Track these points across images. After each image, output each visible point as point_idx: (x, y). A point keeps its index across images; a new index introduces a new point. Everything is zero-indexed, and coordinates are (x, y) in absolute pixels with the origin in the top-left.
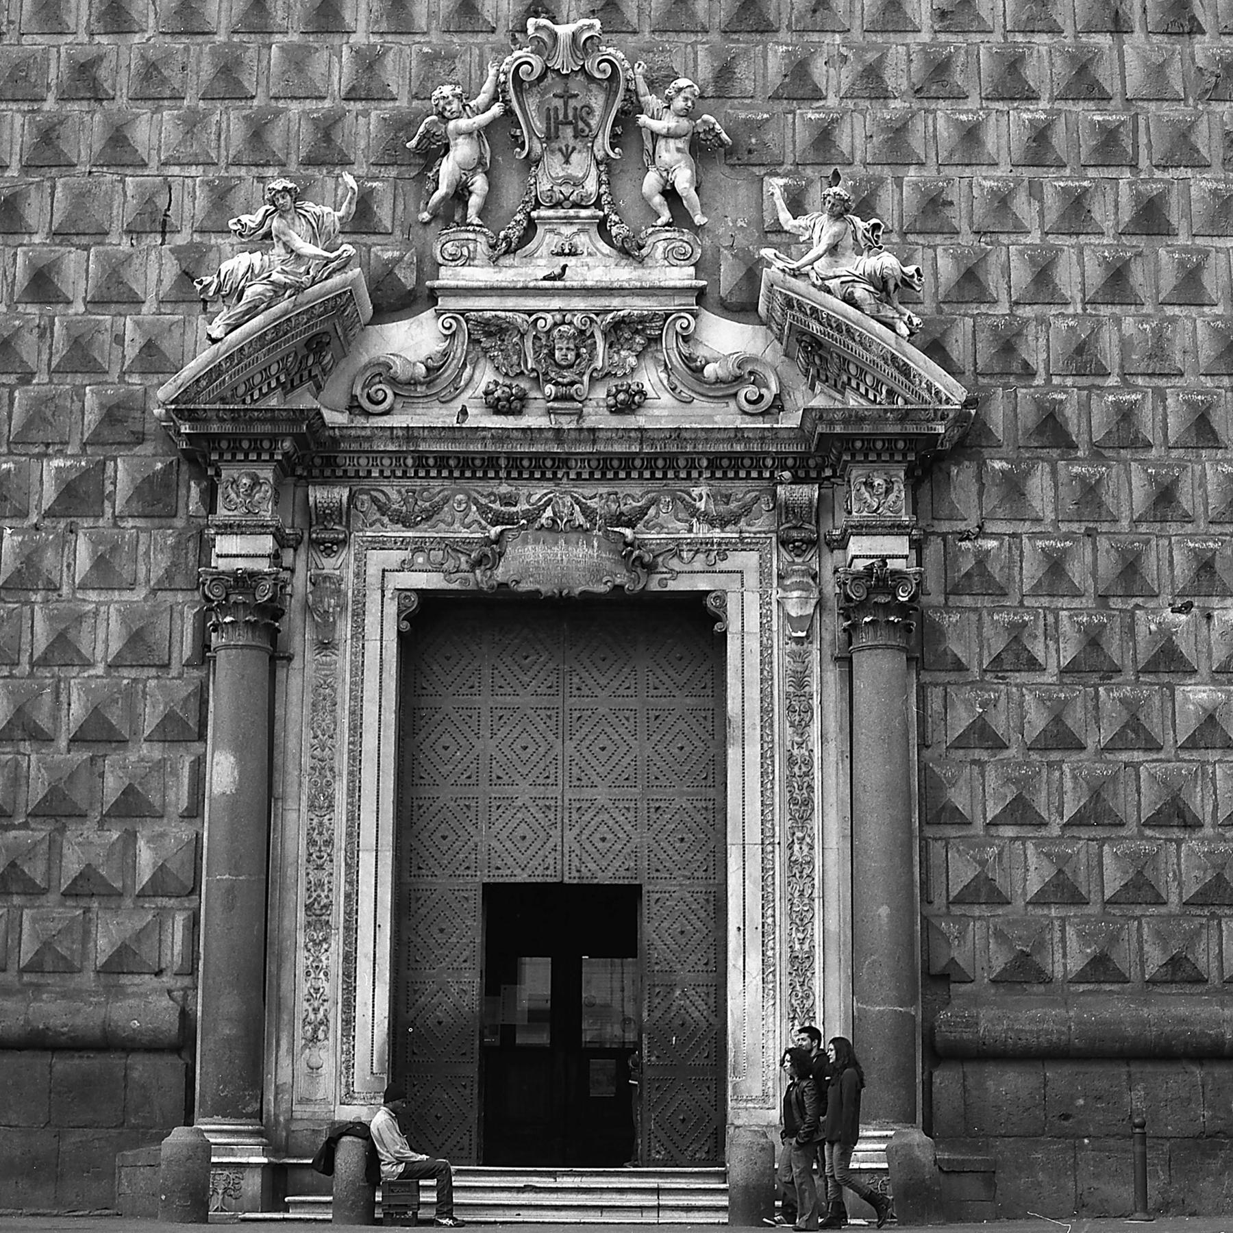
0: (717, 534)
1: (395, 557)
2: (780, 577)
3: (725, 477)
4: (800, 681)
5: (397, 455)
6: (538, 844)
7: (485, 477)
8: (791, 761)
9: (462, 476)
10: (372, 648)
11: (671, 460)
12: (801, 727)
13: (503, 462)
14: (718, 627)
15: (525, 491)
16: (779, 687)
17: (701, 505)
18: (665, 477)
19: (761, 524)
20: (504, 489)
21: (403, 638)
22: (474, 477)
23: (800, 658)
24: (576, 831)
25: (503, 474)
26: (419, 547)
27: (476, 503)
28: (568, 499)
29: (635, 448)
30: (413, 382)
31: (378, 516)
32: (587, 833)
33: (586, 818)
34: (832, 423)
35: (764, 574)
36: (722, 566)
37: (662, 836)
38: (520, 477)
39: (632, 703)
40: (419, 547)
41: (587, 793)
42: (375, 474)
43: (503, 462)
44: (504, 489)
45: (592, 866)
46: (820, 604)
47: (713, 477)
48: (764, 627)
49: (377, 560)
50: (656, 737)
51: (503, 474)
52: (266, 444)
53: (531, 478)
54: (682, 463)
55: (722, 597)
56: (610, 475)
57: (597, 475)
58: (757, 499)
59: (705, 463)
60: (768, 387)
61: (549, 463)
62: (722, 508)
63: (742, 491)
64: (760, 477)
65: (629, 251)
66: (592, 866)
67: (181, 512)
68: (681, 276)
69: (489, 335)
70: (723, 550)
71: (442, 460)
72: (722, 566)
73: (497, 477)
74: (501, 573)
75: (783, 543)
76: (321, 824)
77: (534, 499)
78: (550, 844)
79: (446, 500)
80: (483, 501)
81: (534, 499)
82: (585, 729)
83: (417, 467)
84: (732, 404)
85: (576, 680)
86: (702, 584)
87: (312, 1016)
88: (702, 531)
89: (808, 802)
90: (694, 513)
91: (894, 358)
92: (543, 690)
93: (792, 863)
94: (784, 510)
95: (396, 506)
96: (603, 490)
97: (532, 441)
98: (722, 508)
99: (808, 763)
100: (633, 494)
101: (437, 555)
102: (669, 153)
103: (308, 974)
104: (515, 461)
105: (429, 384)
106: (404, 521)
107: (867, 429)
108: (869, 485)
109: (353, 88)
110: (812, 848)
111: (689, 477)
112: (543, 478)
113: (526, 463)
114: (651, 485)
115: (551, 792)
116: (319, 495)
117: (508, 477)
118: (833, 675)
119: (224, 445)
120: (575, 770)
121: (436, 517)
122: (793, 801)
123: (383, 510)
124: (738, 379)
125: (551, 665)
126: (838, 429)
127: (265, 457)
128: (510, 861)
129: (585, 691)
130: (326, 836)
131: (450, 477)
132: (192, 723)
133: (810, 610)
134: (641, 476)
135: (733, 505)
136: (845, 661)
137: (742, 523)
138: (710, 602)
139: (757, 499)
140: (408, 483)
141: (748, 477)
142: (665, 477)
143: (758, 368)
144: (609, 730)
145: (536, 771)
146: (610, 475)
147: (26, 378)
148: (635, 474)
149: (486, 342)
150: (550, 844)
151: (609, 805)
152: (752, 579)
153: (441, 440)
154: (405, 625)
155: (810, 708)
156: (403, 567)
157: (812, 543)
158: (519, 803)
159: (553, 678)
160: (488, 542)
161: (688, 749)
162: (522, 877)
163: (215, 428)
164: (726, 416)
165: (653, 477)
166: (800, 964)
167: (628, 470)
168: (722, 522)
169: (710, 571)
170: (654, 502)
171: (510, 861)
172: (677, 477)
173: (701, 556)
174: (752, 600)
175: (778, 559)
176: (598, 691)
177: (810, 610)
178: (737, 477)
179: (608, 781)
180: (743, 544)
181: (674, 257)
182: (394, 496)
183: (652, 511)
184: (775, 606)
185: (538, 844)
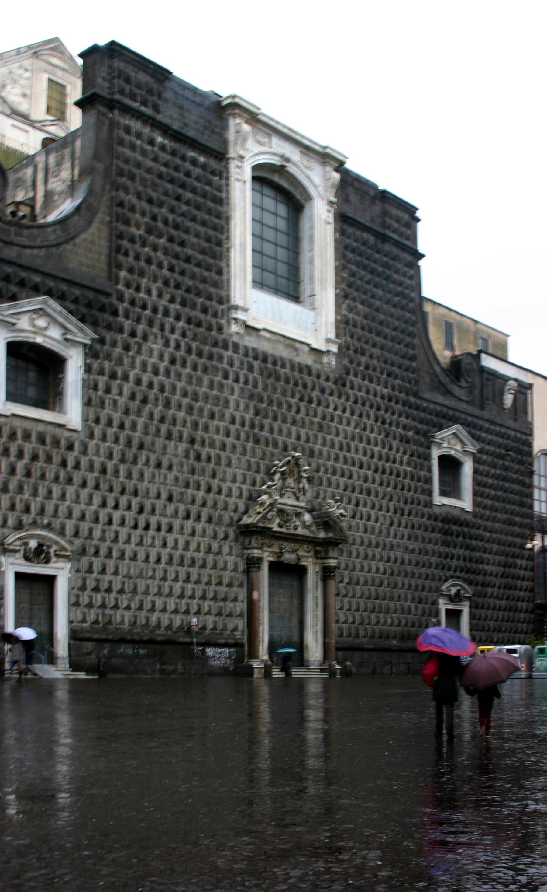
19: (312, 553)
26: (271, 552)
40: (271, 552)
49: (266, 554)
63: (310, 547)
65: (298, 499)
68: (303, 504)
74: (282, 559)
88: (306, 554)
94: (316, 552)
100: (297, 546)
102: (304, 481)
147: (217, 510)
156: (268, 556)
168: (308, 552)
181: (303, 501)
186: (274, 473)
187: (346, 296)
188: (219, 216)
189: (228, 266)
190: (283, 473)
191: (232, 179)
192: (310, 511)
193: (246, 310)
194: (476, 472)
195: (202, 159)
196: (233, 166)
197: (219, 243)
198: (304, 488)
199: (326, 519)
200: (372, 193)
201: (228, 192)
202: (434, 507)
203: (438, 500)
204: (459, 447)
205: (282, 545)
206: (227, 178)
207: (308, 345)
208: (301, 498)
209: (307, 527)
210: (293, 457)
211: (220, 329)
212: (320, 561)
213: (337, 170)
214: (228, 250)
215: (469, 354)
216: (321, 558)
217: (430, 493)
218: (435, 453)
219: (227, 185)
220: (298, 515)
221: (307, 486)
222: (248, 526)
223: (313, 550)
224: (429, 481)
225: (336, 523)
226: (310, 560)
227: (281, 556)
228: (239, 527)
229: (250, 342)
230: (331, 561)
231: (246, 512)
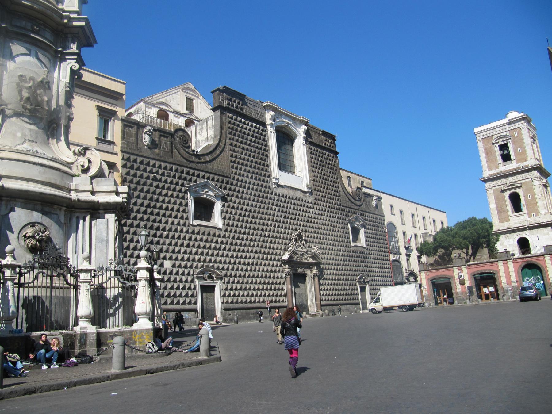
65: (302, 248)
136: (314, 279)
186: (293, 239)
187: (313, 171)
188: (266, 146)
189: (270, 163)
190: (295, 239)
191: (269, 132)
193: (278, 179)
194: (365, 233)
195: (258, 126)
196: (268, 127)
197: (266, 156)
200: (318, 132)
201: (268, 137)
203: (352, 244)
206: (267, 132)
207: (300, 190)
209: (306, 259)
210: (299, 232)
211: (269, 187)
213: (305, 125)
214: (270, 157)
215: (358, 188)
217: (350, 242)
219: (268, 134)
222: (284, 260)
224: (348, 238)
228: (282, 261)
229: (280, 191)
231: (284, 254)
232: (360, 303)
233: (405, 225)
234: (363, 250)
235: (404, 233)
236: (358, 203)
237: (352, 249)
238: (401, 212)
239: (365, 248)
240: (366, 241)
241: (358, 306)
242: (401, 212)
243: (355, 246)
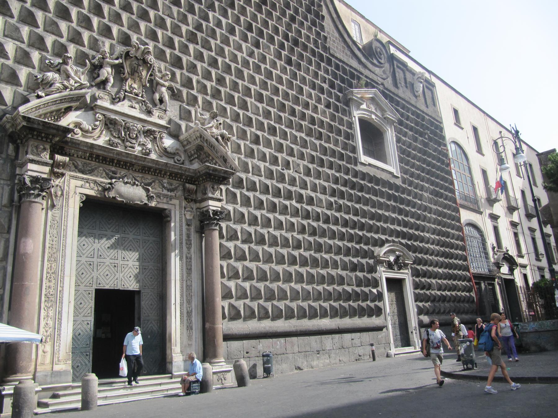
0: (169, 193)
1: (80, 183)
2: (185, 208)
3: (172, 179)
4: (188, 236)
5: (85, 152)
6: (112, 277)
7: (109, 165)
8: (187, 258)
9: (102, 163)
10: (71, 210)
11: (161, 171)
12: (189, 248)
13: (115, 161)
14: (169, 219)
15: (119, 171)
16: (184, 237)
17: (165, 185)
18: (158, 175)
19: (179, 193)
20: (113, 169)
21: (81, 208)
22: (106, 164)
23: (188, 230)
24: (123, 274)
25: (114, 165)
26: (87, 181)
27: (105, 171)
28: (131, 176)
29: (154, 166)
30: (87, 131)
31: (74, 169)
32: (126, 274)
33: (126, 270)
34: (210, 170)
35: (181, 207)
36: (170, 202)
37: (146, 276)
38: (119, 167)
39: (139, 237)
41: (126, 263)
42: (75, 156)
43: (115, 161)
44: (113, 169)
45: (127, 284)
46: (194, 217)
47: (169, 178)
48: (181, 221)
49: (74, 182)
50: (145, 248)
51: (114, 165)
52: (51, 137)
53: (122, 168)
54: (163, 173)
55: (170, 211)
56: (144, 172)
57: (140, 171)
58: (178, 186)
59: (169, 174)
60: (181, 157)
61: (128, 164)
62: (170, 187)
63: (175, 183)
64: (181, 181)
65: (149, 112)
66: (127, 284)
67: (5, 153)
68: (163, 123)
69: (111, 124)
70: (171, 198)
71: (98, 156)
72: (170, 202)
73: (112, 165)
74: (112, 194)
75: (186, 199)
76: (51, 266)
77: (122, 174)
78: (116, 278)
79: (96, 168)
80: (107, 171)
81: (122, 174)
82: (126, 243)
83: (89, 156)
84: (172, 160)
85: (124, 229)
86: (165, 206)
87: (45, 333)
88: (165, 192)
89: (190, 269)
90: (164, 187)
91: (224, 157)
92: (114, 230)
93: (187, 286)
95: (80, 167)
96: (140, 175)
97: (127, 157)
98: (170, 187)
99: (191, 258)
101: (92, 185)
103: (44, 319)
104: (119, 161)
105: (91, 133)
106: (83, 172)
107: (217, 173)
108: (213, 188)
109: (73, 39)
110: (192, 281)
111: (163, 177)
112: (126, 168)
113: (122, 163)
114: (155, 177)
115: (116, 261)
116: (58, 157)
117: (116, 166)
118: (197, 236)
119: (35, 133)
120: (123, 256)
121: (93, 173)
122: (187, 269)
123: (76, 167)
124: (174, 154)
125: (117, 224)
126: (211, 172)
127: (49, 140)
128: (103, 282)
129: (126, 232)
130: (53, 271)
131: (99, 162)
132: (6, 227)
133: (191, 218)
134: (152, 174)
135: (173, 187)
137: (175, 192)
138: (167, 212)
139: (178, 186)
140: (85, 161)
141: (178, 180)
142: (158, 175)
143: (179, 152)
144: (133, 245)
145: (112, 255)
146: (144, 172)
148: (150, 173)
149: (110, 126)
150: (116, 278)
151: (132, 266)
152: (178, 207)
153: (101, 150)
154: (82, 205)
155: (191, 244)
157: (192, 200)
158: (107, 264)
159: (117, 228)
160: (111, 184)
161: (153, 252)
162: (107, 287)
163: (36, 126)
164: (171, 162)
165: (155, 175)
166: (189, 314)
167: (149, 171)
169: (167, 203)
170: (154, 182)
171: (103, 282)
172: (161, 176)
173: (165, 199)
174: (178, 213)
175: (184, 203)
176: (129, 233)
177: (191, 218)
178: (175, 180)
179: (132, 259)
180: (176, 197)
181: (160, 118)
182: (80, 164)
183: (153, 184)
184: (183, 215)
185: (112, 277)
192: (175, 135)
194: (398, 140)
198: (161, 101)
199: (198, 141)
202: (358, 164)
203: (364, 158)
204: (379, 114)
205: (115, 173)
208: (156, 113)
212: (194, 206)
216: (196, 201)
217: (354, 150)
218: (357, 114)
220: (148, 133)
221: (166, 97)
223: (181, 188)
225: (212, 146)
226: (176, 202)
227: (109, 189)
230: (211, 202)
232: (390, 327)
233: (483, 155)
234: (392, 180)
235: (484, 172)
236: (377, 70)
237: (359, 168)
238: (475, 129)
239: (397, 177)
240: (401, 160)
241: (380, 335)
242: (475, 129)
243: (370, 165)
